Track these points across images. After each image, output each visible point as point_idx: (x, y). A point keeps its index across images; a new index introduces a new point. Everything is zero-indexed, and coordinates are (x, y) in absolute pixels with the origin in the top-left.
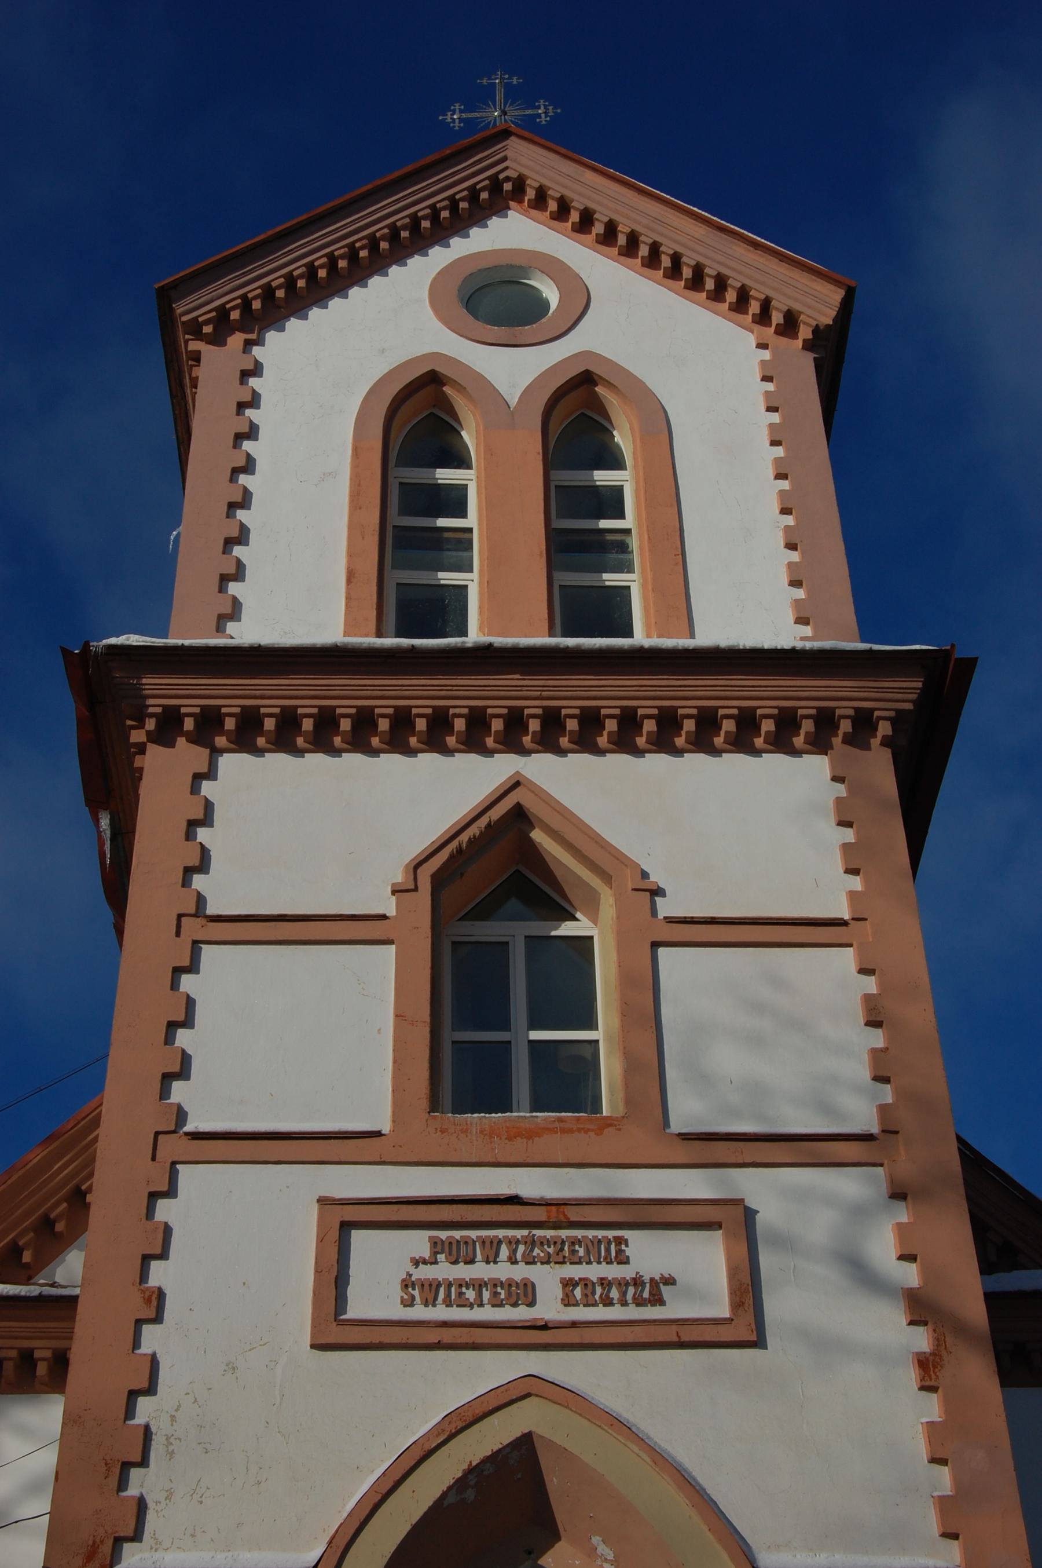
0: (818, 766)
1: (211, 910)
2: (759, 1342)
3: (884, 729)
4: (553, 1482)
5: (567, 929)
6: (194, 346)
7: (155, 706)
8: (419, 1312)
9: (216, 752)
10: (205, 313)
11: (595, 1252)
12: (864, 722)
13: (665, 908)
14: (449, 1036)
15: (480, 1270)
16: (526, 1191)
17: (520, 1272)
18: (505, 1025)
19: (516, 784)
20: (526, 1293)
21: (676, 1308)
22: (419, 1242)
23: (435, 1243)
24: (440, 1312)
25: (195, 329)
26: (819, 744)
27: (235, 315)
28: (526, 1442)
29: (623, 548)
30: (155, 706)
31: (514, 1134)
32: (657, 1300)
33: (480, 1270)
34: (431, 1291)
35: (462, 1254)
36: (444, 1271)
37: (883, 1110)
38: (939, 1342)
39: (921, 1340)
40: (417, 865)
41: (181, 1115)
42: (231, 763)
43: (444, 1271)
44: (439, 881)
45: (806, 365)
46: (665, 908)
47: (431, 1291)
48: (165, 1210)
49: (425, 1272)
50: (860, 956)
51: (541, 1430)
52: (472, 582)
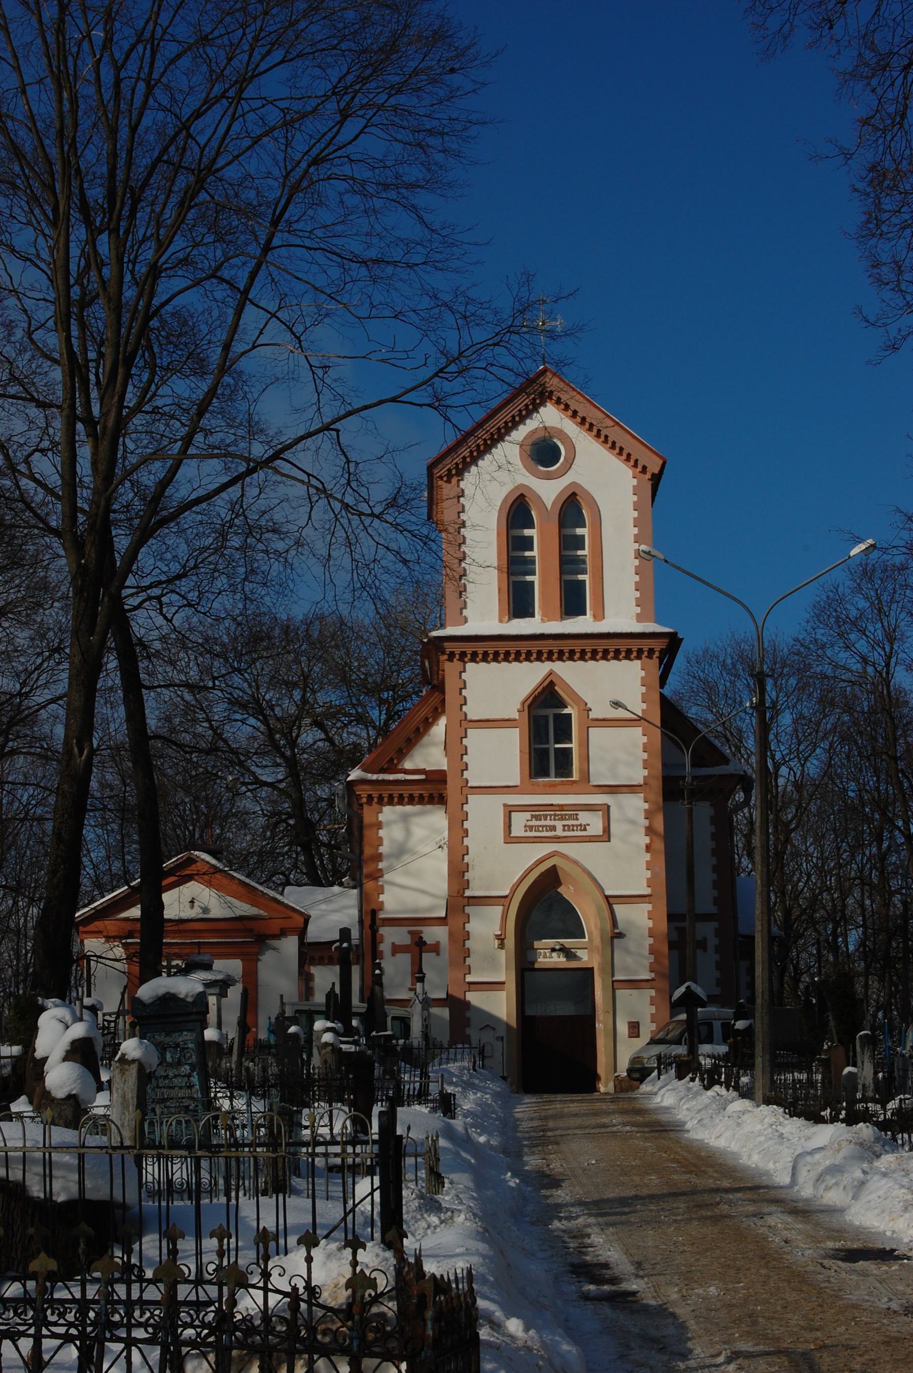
0: (638, 663)
1: (469, 717)
2: (609, 841)
3: (657, 654)
4: (560, 874)
5: (566, 711)
6: (440, 483)
7: (448, 651)
8: (529, 834)
9: (465, 663)
10: (444, 472)
11: (571, 817)
12: (651, 652)
13: (592, 715)
14: (533, 746)
15: (543, 823)
16: (555, 803)
17: (552, 823)
18: (547, 742)
19: (551, 673)
20: (553, 828)
21: (590, 831)
22: (528, 815)
23: (532, 816)
24: (533, 834)
25: (441, 478)
26: (639, 657)
27: (454, 472)
28: (554, 867)
29: (584, 562)
30: (448, 651)
31: (553, 785)
32: (585, 830)
33: (543, 823)
34: (531, 828)
35: (538, 818)
36: (534, 823)
37: (645, 777)
38: (651, 840)
39: (647, 840)
40: (523, 703)
41: (467, 781)
42: (470, 666)
43: (534, 823)
44: (529, 706)
45: (648, 486)
46: (592, 715)
47: (531, 828)
48: (466, 807)
49: (530, 823)
50: (643, 730)
51: (558, 864)
52: (535, 579)
